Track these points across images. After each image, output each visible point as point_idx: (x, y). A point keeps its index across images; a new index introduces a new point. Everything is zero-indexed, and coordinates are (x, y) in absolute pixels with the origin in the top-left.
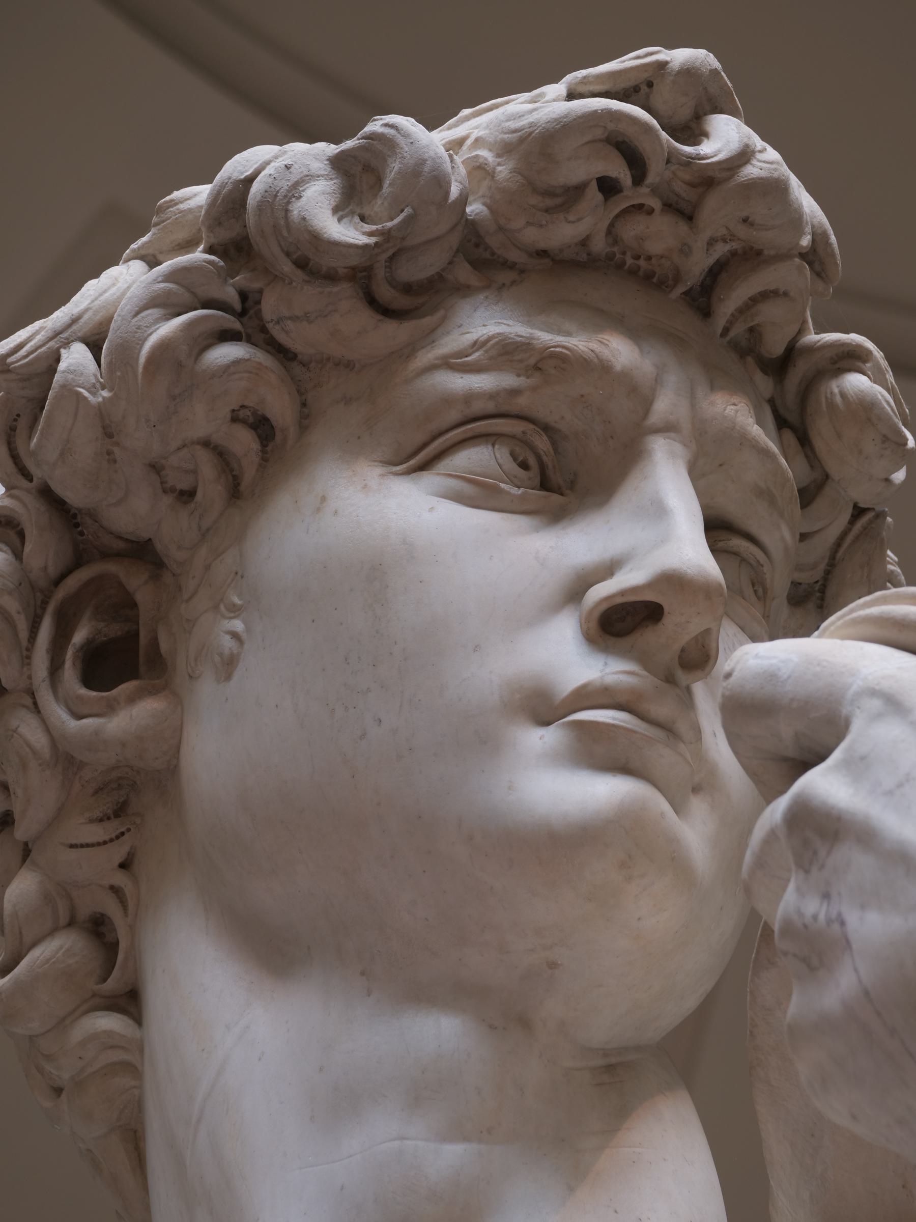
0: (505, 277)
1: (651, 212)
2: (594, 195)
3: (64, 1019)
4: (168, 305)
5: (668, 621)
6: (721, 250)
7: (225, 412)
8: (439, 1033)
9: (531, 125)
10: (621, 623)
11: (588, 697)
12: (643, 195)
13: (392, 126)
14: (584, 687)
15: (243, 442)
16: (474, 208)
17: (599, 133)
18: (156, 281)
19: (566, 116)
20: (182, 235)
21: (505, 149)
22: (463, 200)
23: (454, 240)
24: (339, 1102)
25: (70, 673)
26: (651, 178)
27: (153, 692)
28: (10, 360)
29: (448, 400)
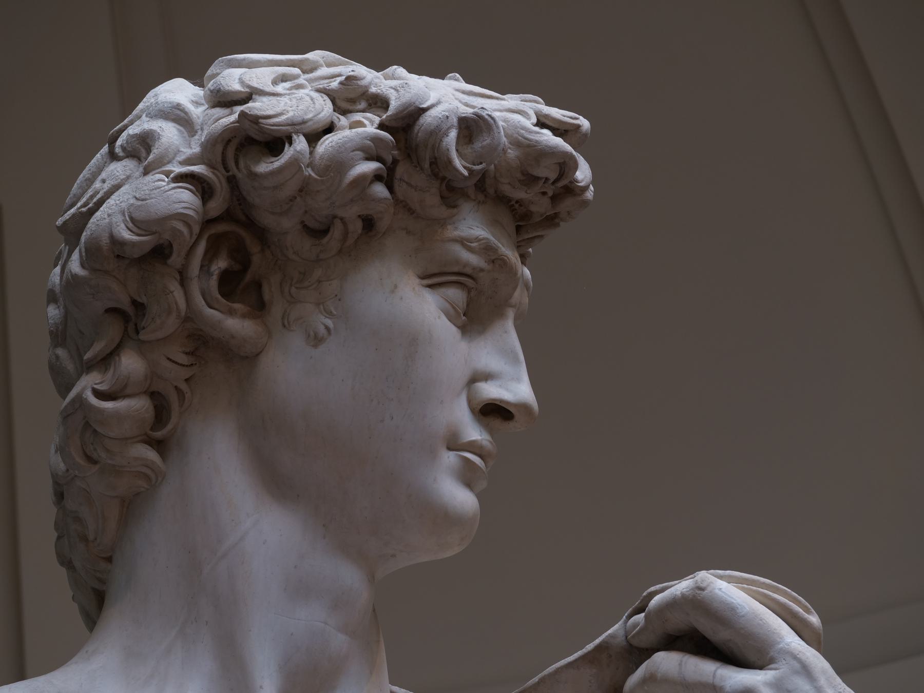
0: (481, 197)
3: (127, 439)
5: (511, 424)
9: (537, 141)
11: (472, 447)
13: (493, 118)
14: (474, 441)
18: (366, 138)
19: (555, 148)
20: (352, 96)
25: (214, 282)
26: (561, 184)
28: (261, 121)
29: (457, 261)
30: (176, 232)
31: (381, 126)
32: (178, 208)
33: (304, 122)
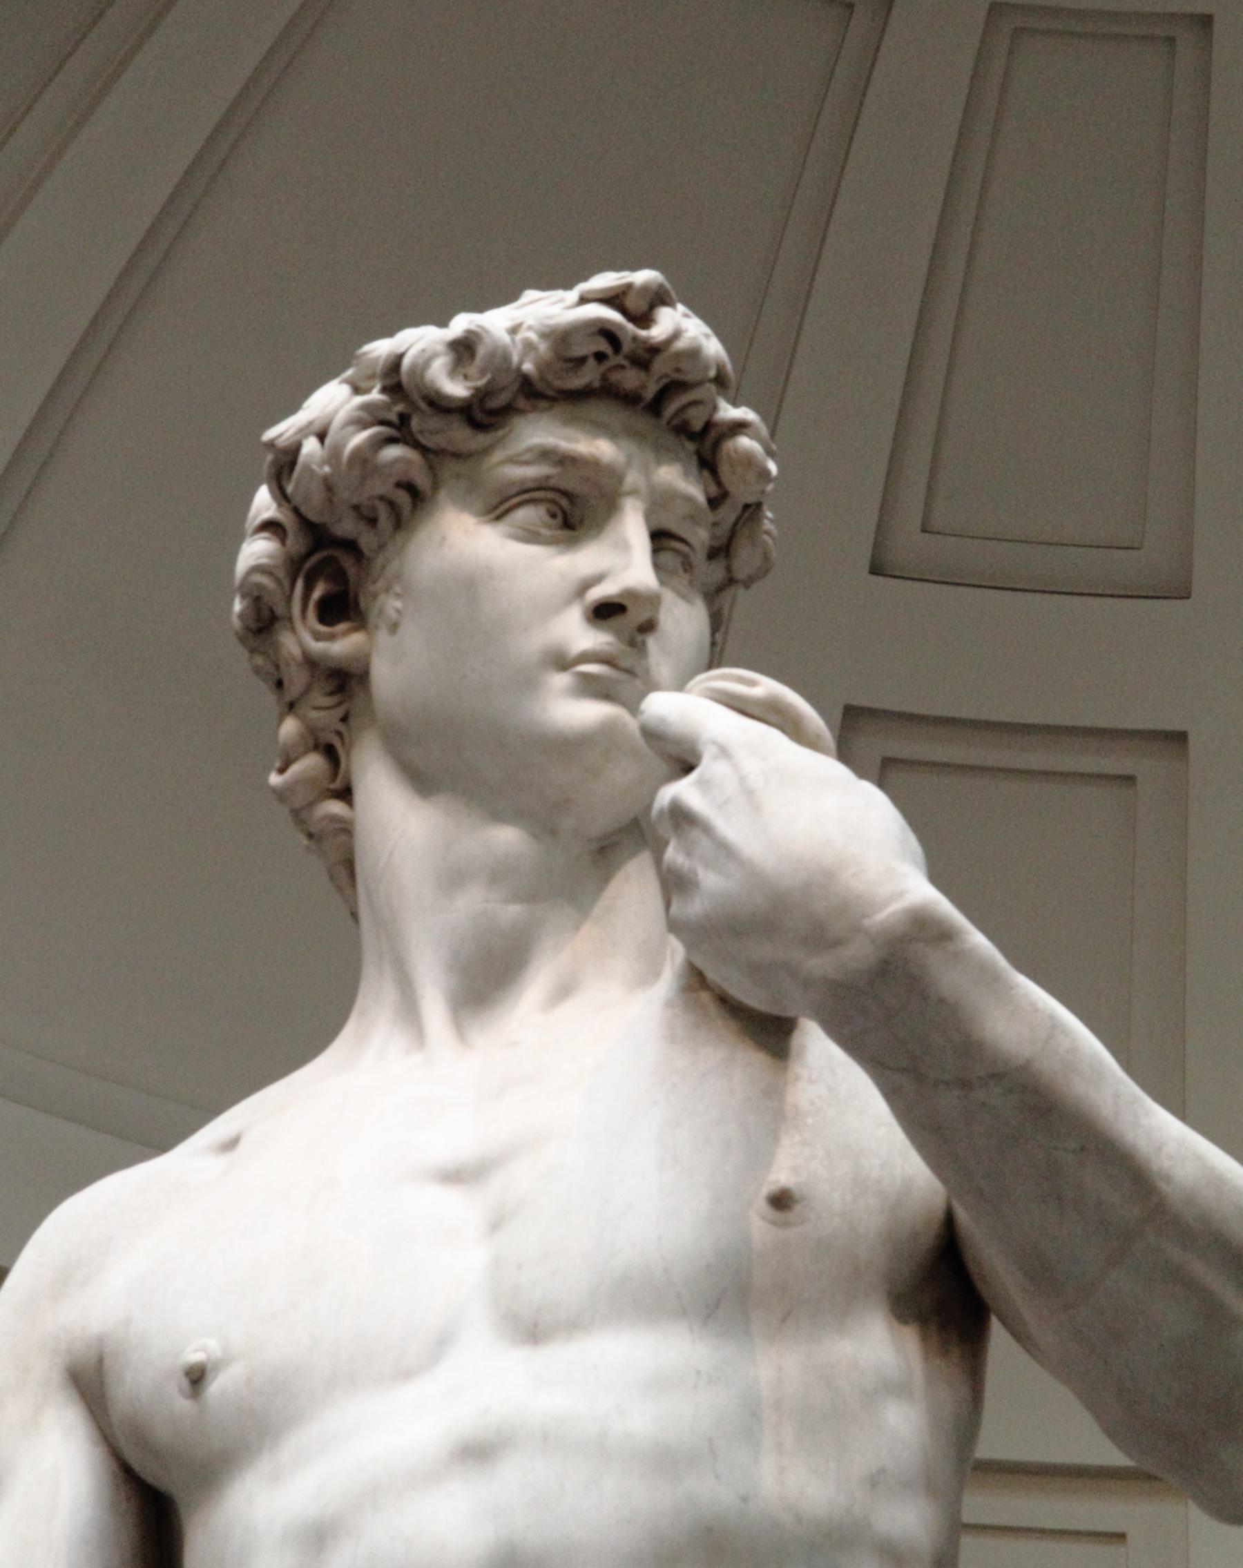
0: (543, 404)
1: (622, 367)
2: (591, 362)
4: (359, 423)
6: (665, 381)
7: (392, 481)
8: (507, 838)
10: (604, 612)
11: (585, 657)
12: (619, 360)
15: (403, 498)
16: (528, 367)
17: (593, 329)
21: (544, 335)
22: (521, 362)
23: (516, 386)
24: (453, 879)
27: (356, 629)
29: (513, 483)
30: (259, 586)
31: (384, 390)
32: (252, 562)
33: (310, 423)
